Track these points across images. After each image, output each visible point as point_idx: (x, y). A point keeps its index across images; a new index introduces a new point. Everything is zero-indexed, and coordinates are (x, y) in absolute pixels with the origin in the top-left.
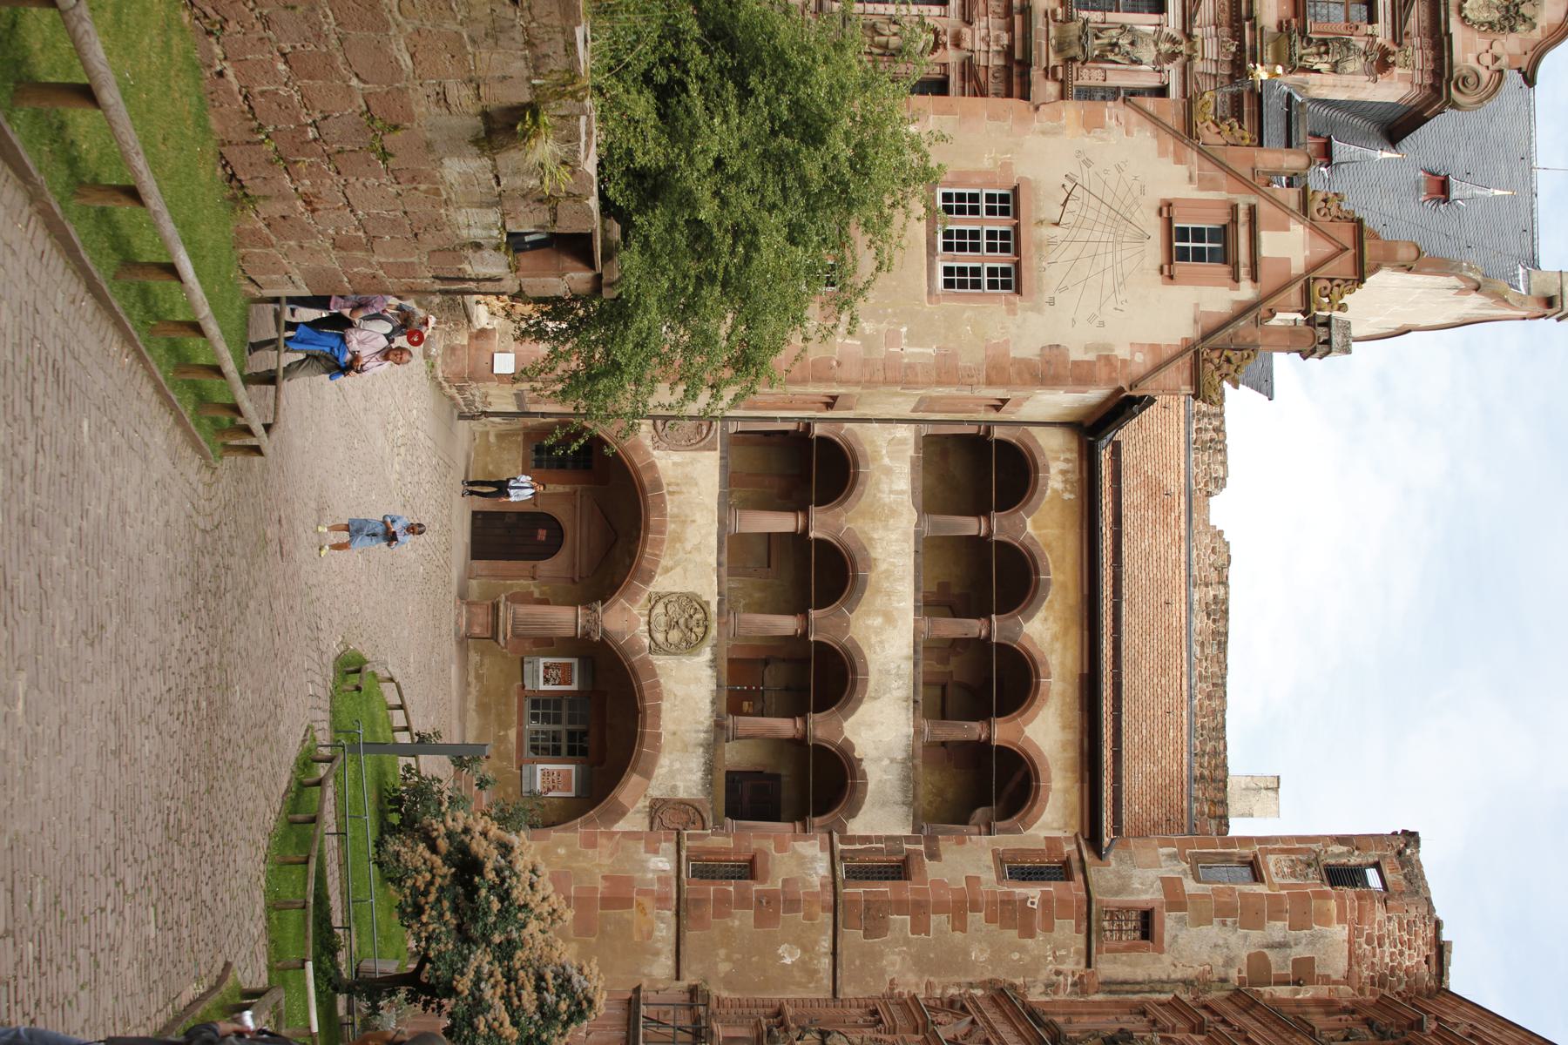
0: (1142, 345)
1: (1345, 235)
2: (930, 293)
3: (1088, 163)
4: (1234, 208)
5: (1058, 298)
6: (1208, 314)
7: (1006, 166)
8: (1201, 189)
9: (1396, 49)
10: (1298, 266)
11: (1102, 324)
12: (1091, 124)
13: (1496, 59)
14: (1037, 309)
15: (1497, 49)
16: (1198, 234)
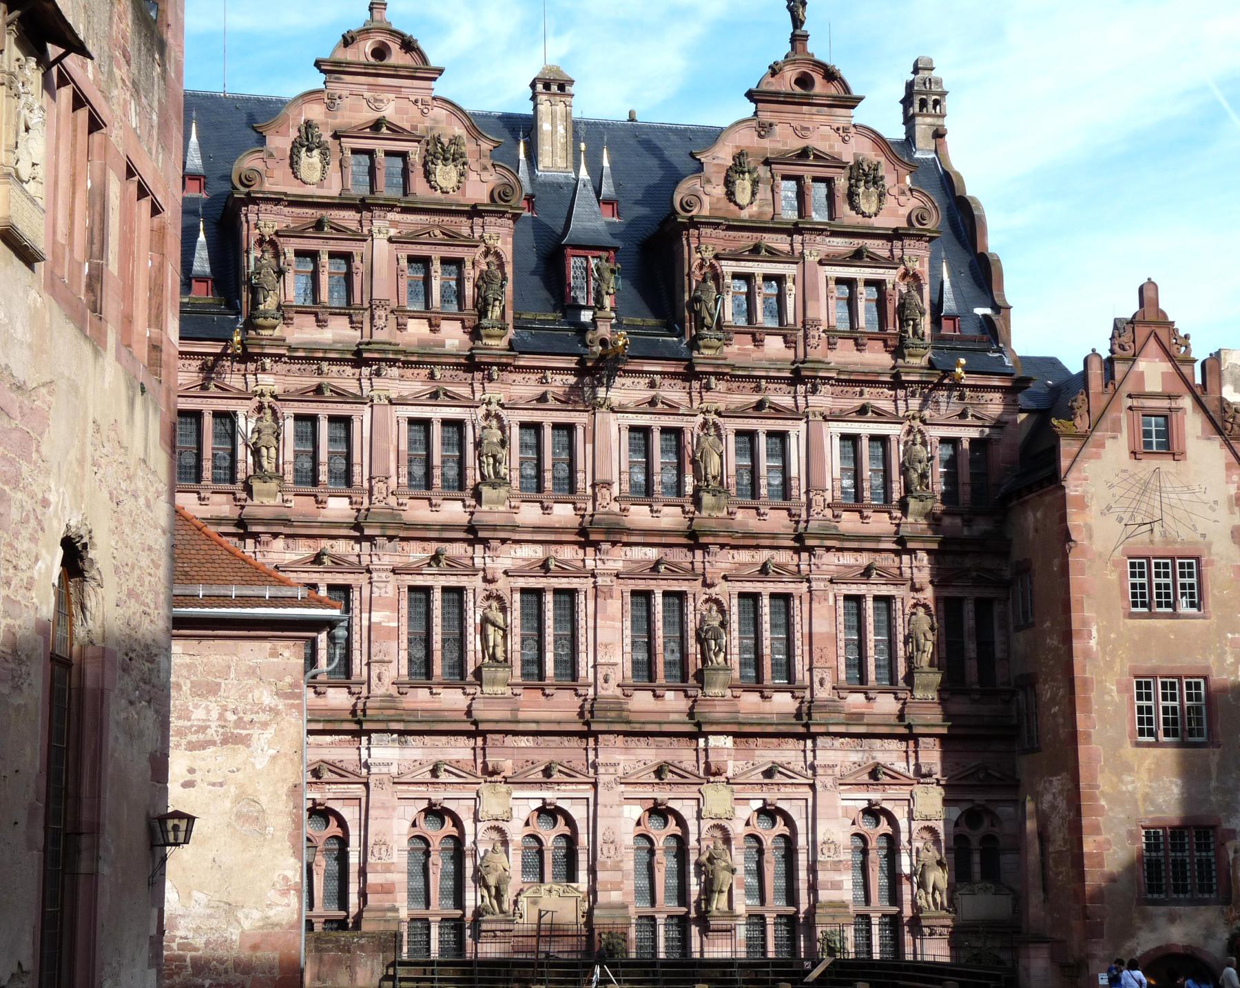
0: (1227, 476)
1: (1142, 332)
2: (1204, 618)
3: (1109, 508)
4: (1130, 408)
5: (1201, 531)
6: (1203, 431)
7: (1116, 564)
8: (1120, 430)
9: (902, 267)
10: (1167, 367)
11: (1216, 502)
12: (1082, 504)
13: (903, 193)
14: (1209, 545)
15: (894, 191)
16: (1147, 434)
